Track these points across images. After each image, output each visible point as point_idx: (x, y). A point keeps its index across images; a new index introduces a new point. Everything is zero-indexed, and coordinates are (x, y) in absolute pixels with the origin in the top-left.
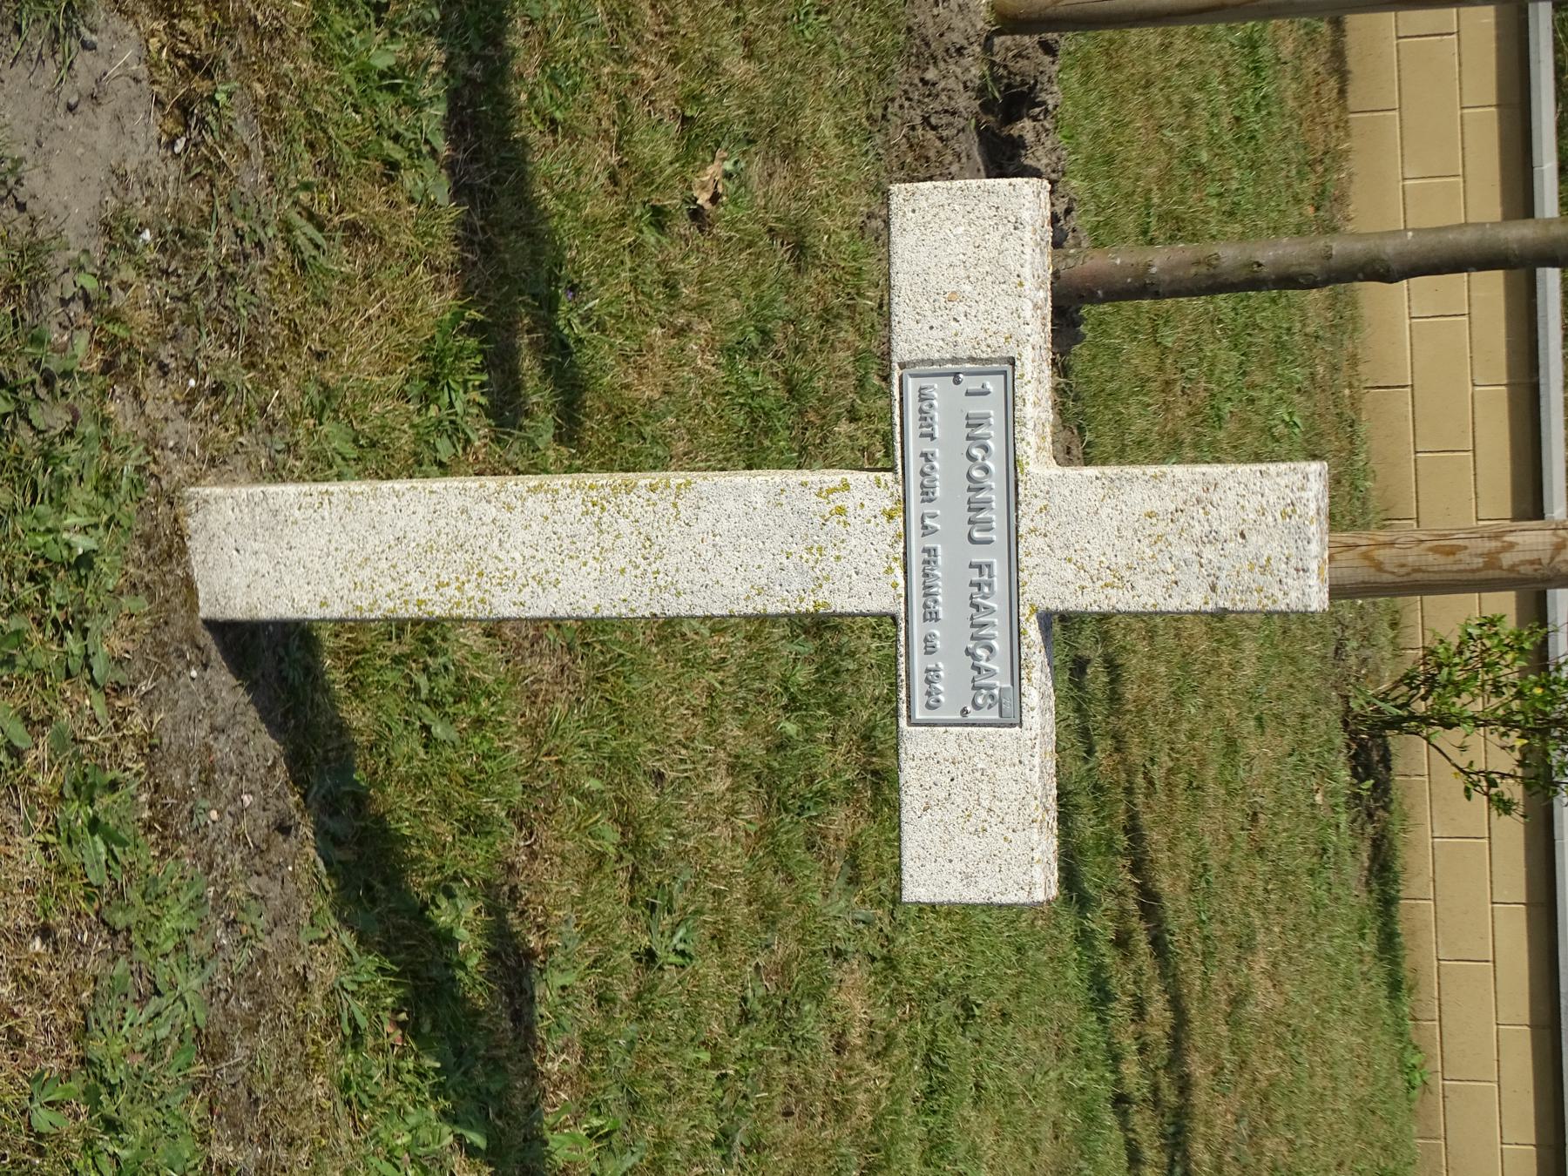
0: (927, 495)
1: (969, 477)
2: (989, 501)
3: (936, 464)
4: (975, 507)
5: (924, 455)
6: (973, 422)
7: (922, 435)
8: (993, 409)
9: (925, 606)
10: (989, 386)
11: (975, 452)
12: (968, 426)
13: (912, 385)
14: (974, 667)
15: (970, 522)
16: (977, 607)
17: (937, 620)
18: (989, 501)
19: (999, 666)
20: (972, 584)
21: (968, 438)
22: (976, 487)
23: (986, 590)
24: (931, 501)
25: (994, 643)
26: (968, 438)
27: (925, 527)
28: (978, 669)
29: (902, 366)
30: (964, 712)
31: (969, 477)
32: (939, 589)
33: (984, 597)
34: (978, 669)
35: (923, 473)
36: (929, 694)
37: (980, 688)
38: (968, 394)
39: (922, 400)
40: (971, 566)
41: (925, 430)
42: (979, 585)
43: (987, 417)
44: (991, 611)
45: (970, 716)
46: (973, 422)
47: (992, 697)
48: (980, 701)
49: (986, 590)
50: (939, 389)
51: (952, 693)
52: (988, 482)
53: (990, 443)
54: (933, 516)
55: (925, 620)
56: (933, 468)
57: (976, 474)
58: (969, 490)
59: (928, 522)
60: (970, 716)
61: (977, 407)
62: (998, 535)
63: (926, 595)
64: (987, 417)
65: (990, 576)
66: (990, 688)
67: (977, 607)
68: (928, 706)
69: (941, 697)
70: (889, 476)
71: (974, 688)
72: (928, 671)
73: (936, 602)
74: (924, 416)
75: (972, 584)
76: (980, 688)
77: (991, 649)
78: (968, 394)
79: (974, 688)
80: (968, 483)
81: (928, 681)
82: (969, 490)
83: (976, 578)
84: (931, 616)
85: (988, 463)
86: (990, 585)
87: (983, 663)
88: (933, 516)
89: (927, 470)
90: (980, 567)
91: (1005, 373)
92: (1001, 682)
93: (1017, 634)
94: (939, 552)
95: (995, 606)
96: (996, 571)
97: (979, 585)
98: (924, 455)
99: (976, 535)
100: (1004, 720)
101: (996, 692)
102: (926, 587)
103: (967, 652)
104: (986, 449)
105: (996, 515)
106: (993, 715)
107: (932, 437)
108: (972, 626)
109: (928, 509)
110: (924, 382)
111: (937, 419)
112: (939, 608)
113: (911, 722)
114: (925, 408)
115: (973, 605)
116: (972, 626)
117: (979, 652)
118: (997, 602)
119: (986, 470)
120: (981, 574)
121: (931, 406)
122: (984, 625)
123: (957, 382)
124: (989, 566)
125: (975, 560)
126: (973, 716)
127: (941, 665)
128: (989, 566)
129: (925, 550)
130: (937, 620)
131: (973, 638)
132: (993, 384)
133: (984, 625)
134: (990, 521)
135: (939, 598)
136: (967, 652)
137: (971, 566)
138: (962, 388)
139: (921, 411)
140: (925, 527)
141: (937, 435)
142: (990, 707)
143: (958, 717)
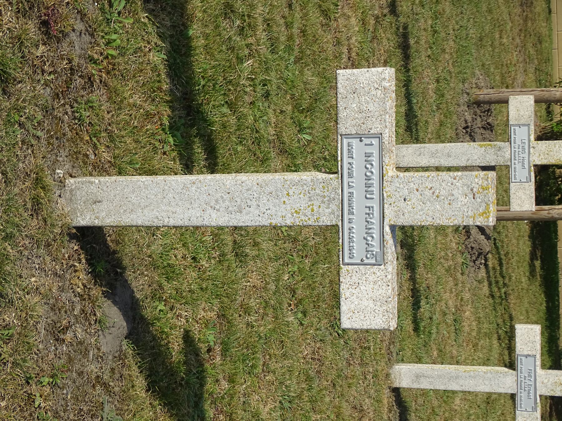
0: (350, 175)
1: (366, 175)
2: (373, 184)
3: (354, 166)
4: (368, 186)
5: (349, 163)
6: (368, 155)
7: (349, 157)
8: (375, 151)
9: (349, 210)
10: (373, 142)
11: (368, 166)
12: (366, 156)
13: (345, 141)
14: (366, 244)
15: (366, 191)
16: (368, 222)
17: (353, 214)
18: (373, 184)
19: (375, 243)
20: (366, 214)
21: (366, 161)
22: (368, 178)
23: (371, 216)
24: (352, 177)
25: (374, 235)
26: (366, 161)
27: (349, 186)
28: (368, 244)
29: (341, 135)
30: (362, 260)
31: (366, 175)
32: (355, 205)
33: (371, 218)
34: (368, 244)
35: (349, 169)
36: (350, 254)
37: (369, 251)
38: (366, 145)
39: (349, 146)
40: (366, 207)
41: (350, 156)
42: (369, 214)
43: (372, 153)
44: (373, 224)
45: (365, 262)
46: (368, 155)
47: (373, 254)
48: (368, 256)
49: (371, 216)
50: (355, 142)
51: (359, 252)
52: (373, 177)
53: (373, 163)
54: (353, 182)
55: (349, 214)
56: (352, 167)
57: (368, 174)
58: (366, 179)
59: (350, 184)
60: (365, 262)
61: (369, 150)
62: (376, 196)
63: (349, 207)
64: (372, 153)
65: (373, 211)
66: (372, 251)
67: (368, 222)
68: (350, 258)
69: (355, 255)
70: (336, 175)
71: (366, 251)
72: (349, 219)
73: (353, 208)
74: (349, 151)
75: (366, 214)
76: (369, 251)
77: (373, 237)
78: (366, 145)
79: (366, 251)
80: (365, 177)
81: (350, 250)
82: (366, 179)
83: (368, 212)
84: (351, 213)
85: (373, 170)
86: (373, 214)
87: (370, 242)
88: (353, 182)
89: (350, 168)
90: (369, 207)
91: (379, 138)
92: (376, 249)
93: (382, 235)
94: (354, 193)
95: (374, 222)
96: (375, 209)
97: (369, 214)
98: (349, 163)
99: (368, 196)
100: (377, 263)
101: (374, 253)
102: (349, 204)
103: (364, 238)
104: (372, 165)
105: (375, 189)
106: (373, 261)
107: (352, 158)
108: (366, 229)
109: (350, 180)
110: (350, 140)
111: (354, 151)
112: (354, 211)
113: (344, 264)
114: (350, 149)
115: (366, 221)
116: (366, 229)
117: (369, 238)
118: (375, 221)
119: (372, 173)
120: (370, 210)
121: (352, 148)
122: (370, 229)
123: (361, 141)
124: (372, 207)
125: (368, 205)
126: (366, 261)
127: (355, 245)
128: (372, 207)
129: (349, 193)
130: (353, 214)
131: (366, 233)
132: (375, 142)
133: (370, 229)
134: (373, 191)
135: (354, 208)
136: (364, 238)
137: (366, 207)
138: (363, 143)
139: (349, 150)
140: (349, 186)
141: (354, 157)
142: (372, 258)
143: (359, 261)
